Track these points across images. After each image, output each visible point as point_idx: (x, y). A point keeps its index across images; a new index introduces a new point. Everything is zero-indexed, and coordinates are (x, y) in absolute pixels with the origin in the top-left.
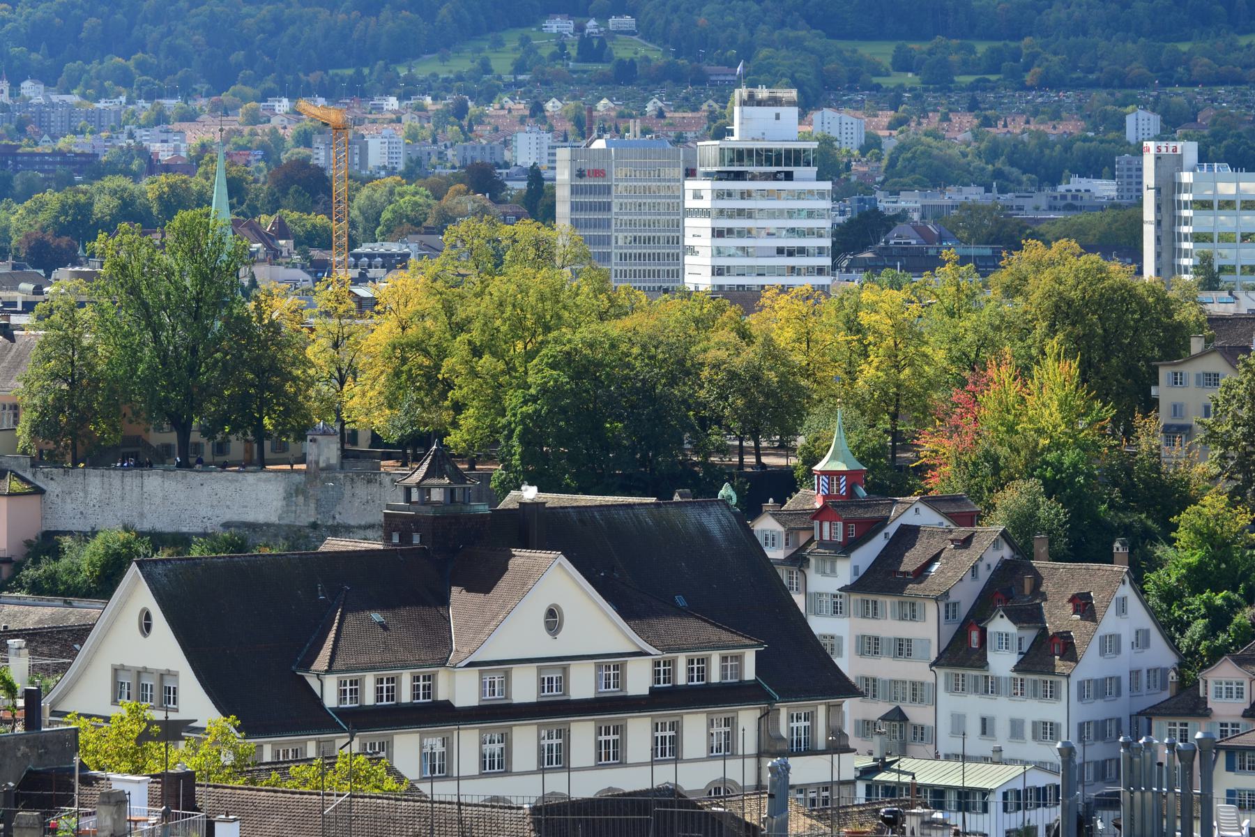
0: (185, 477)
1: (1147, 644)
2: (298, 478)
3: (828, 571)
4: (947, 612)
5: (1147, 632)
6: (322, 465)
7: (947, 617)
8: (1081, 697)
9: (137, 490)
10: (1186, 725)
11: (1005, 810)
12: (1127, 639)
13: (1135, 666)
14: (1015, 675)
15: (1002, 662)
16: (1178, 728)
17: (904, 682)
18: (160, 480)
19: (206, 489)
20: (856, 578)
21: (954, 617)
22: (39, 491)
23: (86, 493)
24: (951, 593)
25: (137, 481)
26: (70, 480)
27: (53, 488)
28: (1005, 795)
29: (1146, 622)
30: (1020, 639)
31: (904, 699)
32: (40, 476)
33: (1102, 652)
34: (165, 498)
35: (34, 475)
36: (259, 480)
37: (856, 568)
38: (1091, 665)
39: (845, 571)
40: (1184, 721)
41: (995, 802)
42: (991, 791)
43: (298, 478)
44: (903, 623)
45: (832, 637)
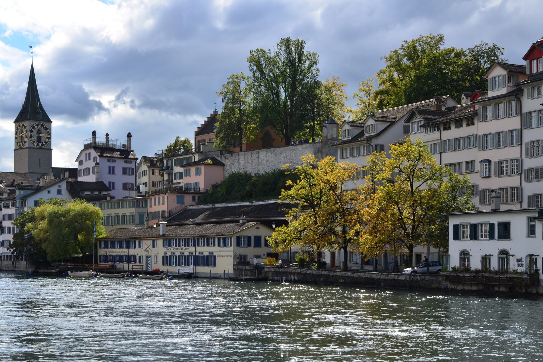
0: (274, 151)
2: (319, 145)
3: (536, 95)
6: (329, 137)
9: (257, 159)
18: (265, 153)
19: (283, 155)
22: (223, 165)
23: (239, 163)
25: (257, 155)
26: (233, 158)
27: (227, 162)
32: (223, 158)
34: (267, 161)
35: (221, 158)
36: (303, 148)
43: (319, 145)
45: (538, 141)
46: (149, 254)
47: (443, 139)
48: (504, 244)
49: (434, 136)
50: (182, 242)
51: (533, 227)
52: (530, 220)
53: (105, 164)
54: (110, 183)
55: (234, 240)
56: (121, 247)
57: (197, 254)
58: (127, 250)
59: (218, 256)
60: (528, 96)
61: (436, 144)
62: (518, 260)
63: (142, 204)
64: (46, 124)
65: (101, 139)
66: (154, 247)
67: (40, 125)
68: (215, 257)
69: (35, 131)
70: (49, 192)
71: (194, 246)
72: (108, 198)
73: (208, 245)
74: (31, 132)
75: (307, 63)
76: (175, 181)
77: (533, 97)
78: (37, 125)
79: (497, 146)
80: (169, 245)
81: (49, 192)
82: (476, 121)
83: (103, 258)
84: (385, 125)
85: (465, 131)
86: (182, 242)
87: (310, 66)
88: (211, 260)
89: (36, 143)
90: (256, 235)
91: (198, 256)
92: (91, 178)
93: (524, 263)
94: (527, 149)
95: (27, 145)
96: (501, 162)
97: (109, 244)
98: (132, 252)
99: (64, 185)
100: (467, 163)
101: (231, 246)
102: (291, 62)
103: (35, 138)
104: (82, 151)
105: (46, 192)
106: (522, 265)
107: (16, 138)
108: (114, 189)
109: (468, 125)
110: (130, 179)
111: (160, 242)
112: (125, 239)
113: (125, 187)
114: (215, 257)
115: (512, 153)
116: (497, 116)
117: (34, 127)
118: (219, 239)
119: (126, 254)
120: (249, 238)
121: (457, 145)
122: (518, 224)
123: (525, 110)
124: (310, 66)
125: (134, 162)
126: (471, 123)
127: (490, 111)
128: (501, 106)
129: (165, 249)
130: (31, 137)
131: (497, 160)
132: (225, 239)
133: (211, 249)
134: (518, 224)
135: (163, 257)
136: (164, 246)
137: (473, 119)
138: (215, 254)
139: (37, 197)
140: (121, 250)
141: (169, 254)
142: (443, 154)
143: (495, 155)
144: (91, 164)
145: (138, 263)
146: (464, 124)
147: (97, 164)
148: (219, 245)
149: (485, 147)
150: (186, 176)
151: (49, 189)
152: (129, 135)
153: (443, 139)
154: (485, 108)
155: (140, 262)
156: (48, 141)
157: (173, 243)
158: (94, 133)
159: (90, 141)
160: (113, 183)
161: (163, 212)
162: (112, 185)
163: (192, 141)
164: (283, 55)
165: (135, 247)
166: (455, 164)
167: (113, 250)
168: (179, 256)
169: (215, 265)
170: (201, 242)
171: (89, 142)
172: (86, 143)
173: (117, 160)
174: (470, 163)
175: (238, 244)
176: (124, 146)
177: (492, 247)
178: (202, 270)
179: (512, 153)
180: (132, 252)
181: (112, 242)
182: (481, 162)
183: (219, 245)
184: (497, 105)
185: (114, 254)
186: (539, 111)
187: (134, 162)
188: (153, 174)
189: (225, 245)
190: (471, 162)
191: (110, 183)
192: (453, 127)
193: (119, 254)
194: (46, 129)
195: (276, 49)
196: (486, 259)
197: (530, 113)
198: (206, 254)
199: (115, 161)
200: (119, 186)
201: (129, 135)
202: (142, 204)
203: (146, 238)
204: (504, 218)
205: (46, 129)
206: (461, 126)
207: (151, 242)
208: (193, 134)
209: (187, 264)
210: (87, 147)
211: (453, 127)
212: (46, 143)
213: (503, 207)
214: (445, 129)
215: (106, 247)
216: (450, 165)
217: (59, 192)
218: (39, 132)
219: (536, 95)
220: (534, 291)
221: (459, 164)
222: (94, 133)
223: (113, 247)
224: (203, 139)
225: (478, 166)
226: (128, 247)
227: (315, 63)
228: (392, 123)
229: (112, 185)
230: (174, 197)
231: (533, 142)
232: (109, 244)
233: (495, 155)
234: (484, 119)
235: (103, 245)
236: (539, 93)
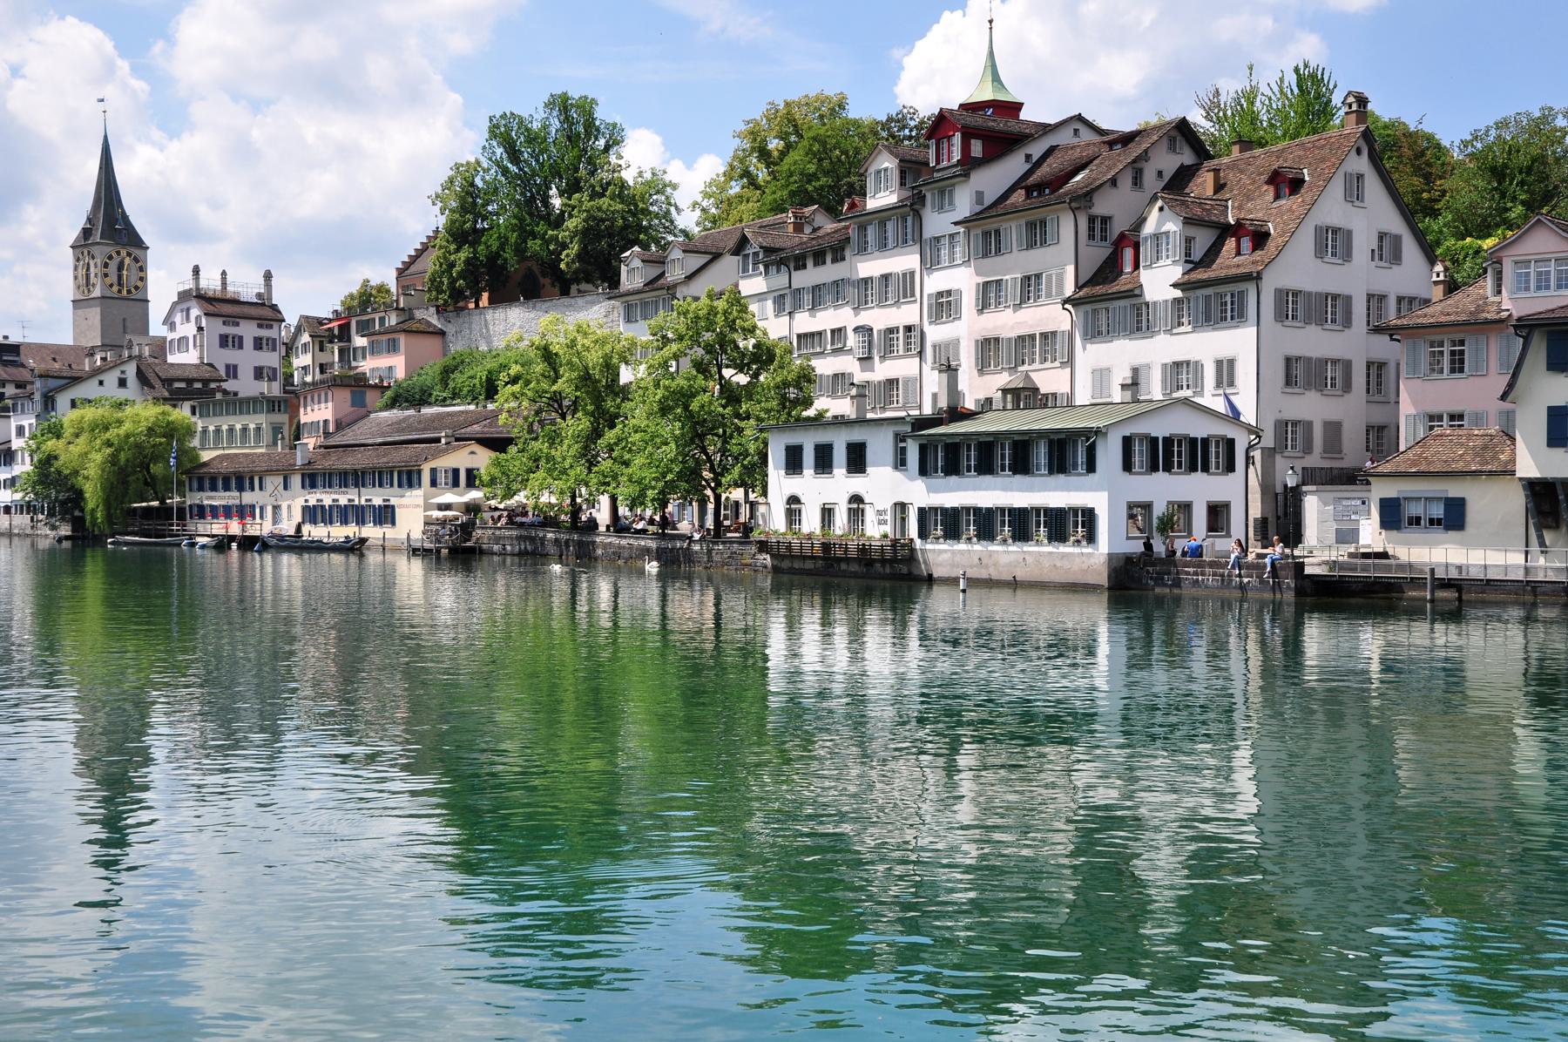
1: (1396, 258)
4: (1091, 229)
5: (1397, 239)
7: (1091, 237)
8: (1281, 315)
10: (1462, 343)
11: (1127, 466)
12: (1363, 243)
13: (1378, 288)
14: (1178, 293)
15: (1159, 280)
16: (1446, 349)
17: (1032, 337)
20: (979, 208)
21: (1104, 238)
24: (1097, 198)
28: (1127, 442)
29: (1394, 223)
30: (1189, 241)
31: (1033, 361)
33: (1320, 251)
37: (980, 196)
38: (1296, 267)
39: (964, 202)
40: (1458, 337)
41: (1109, 454)
42: (1097, 432)
44: (1032, 252)
45: (949, 293)
47: (794, 286)
48: (857, 484)
49: (781, 280)
50: (336, 480)
51: (904, 450)
52: (900, 438)
53: (218, 327)
54: (228, 367)
55: (426, 477)
56: (227, 488)
60: (933, 207)
61: (783, 296)
62: (879, 513)
64: (136, 252)
65: (210, 282)
66: (286, 488)
67: (124, 253)
69: (113, 265)
70: (101, 383)
72: (219, 396)
74: (106, 265)
75: (601, 143)
76: (354, 364)
77: (941, 208)
78: (118, 253)
79: (883, 301)
80: (313, 486)
81: (101, 383)
82: (847, 253)
83: (195, 510)
84: (699, 260)
85: (828, 272)
86: (336, 480)
87: (607, 149)
88: (386, 515)
89: (115, 288)
90: (470, 466)
92: (190, 357)
93: (888, 517)
94: (930, 306)
95: (97, 293)
96: (891, 331)
97: (207, 484)
98: (248, 498)
99: (131, 370)
100: (833, 331)
101: (420, 485)
102: (572, 138)
103: (113, 278)
104: (175, 304)
105: (95, 381)
106: (885, 522)
107: (76, 278)
108: (235, 377)
109: (834, 261)
110: (271, 359)
111: (296, 480)
113: (259, 373)
115: (906, 314)
116: (883, 246)
117: (110, 258)
118: (400, 473)
119: (237, 502)
120: (456, 472)
121: (818, 297)
122: (880, 445)
123: (927, 235)
124: (607, 149)
125: (276, 325)
126: (839, 257)
127: (871, 233)
128: (890, 226)
130: (106, 275)
131: (883, 327)
132: (409, 473)
134: (880, 445)
137: (843, 249)
139: (79, 392)
141: (312, 502)
142: (798, 316)
143: (879, 318)
144: (189, 330)
145: (258, 520)
146: (829, 259)
147: (200, 329)
148: (400, 486)
149: (860, 305)
150: (372, 353)
151: (101, 378)
152: (268, 276)
153: (794, 286)
154: (862, 228)
155: (261, 517)
156: (139, 284)
157: (319, 481)
158: (196, 271)
159: (190, 285)
160: (235, 367)
161: (326, 421)
162: (232, 371)
163: (394, 289)
164: (555, 124)
166: (812, 334)
169: (393, 523)
170: (368, 479)
171: (187, 287)
172: (181, 289)
173: (242, 322)
174: (838, 333)
175: (434, 483)
176: (259, 295)
177: (839, 486)
178: (371, 532)
179: (906, 314)
182: (856, 330)
183: (400, 486)
184: (883, 224)
186: (952, 236)
187: (276, 325)
188: (321, 350)
189: (410, 486)
190: (840, 330)
191: (228, 367)
192: (810, 263)
193: (223, 503)
194: (136, 260)
195: (541, 114)
196: (827, 513)
197: (938, 239)
199: (237, 324)
200: (246, 373)
201: (268, 276)
203: (270, 472)
204: (856, 435)
205: (136, 260)
206: (804, 267)
207: (281, 479)
208: (394, 274)
209: (345, 522)
210: (184, 296)
211: (810, 263)
212: (137, 288)
213: (870, 416)
214: (796, 269)
215: (201, 489)
216: (806, 335)
217: (122, 383)
218: (120, 267)
219: (947, 207)
220: (905, 570)
221: (820, 333)
222: (196, 271)
223: (214, 488)
225: (852, 340)
226: (241, 489)
227: (616, 143)
228: (716, 256)
229: (232, 371)
230: (345, 395)
231: (940, 294)
232: (207, 484)
233: (879, 318)
234: (863, 250)
235: (195, 485)
236: (951, 203)
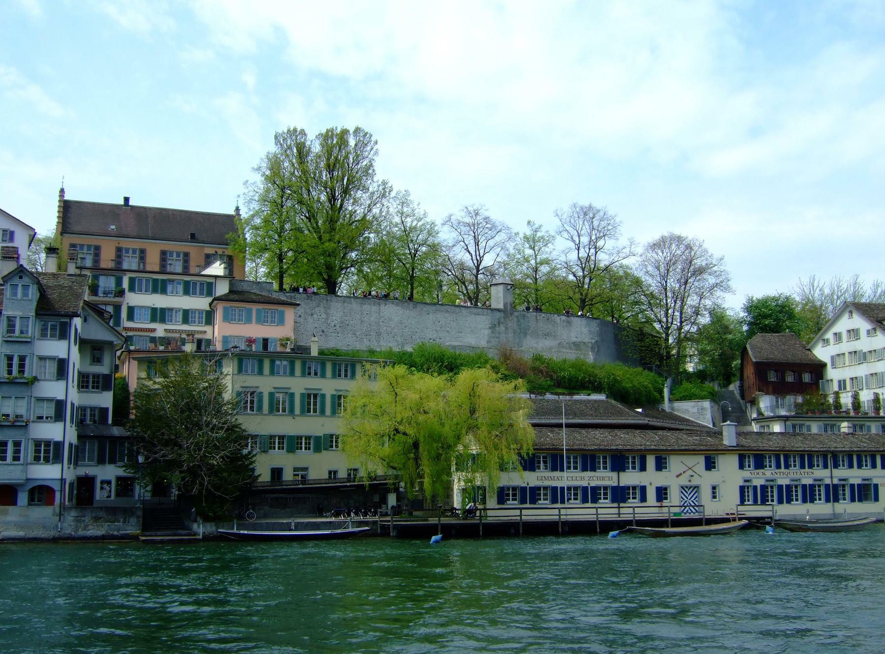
46: (695, 482)
57: (836, 481)
58: (614, 475)
59: (883, 485)
63: (346, 371)
68: (876, 486)
71: (825, 466)
73: (860, 466)
91: (835, 487)
98: (630, 478)
112: (832, 452)
114: (876, 486)
129: (746, 474)
133: (867, 472)
135: (742, 489)
136: (741, 467)
138: (875, 481)
140: (589, 474)
165: (643, 468)
167: (557, 474)
168: (788, 486)
169: (876, 499)
180: (630, 478)
181: (755, 456)
185: (559, 484)
198: (857, 481)
202: (346, 371)
207: (701, 460)
224: (97, 244)
